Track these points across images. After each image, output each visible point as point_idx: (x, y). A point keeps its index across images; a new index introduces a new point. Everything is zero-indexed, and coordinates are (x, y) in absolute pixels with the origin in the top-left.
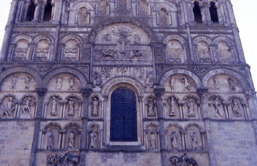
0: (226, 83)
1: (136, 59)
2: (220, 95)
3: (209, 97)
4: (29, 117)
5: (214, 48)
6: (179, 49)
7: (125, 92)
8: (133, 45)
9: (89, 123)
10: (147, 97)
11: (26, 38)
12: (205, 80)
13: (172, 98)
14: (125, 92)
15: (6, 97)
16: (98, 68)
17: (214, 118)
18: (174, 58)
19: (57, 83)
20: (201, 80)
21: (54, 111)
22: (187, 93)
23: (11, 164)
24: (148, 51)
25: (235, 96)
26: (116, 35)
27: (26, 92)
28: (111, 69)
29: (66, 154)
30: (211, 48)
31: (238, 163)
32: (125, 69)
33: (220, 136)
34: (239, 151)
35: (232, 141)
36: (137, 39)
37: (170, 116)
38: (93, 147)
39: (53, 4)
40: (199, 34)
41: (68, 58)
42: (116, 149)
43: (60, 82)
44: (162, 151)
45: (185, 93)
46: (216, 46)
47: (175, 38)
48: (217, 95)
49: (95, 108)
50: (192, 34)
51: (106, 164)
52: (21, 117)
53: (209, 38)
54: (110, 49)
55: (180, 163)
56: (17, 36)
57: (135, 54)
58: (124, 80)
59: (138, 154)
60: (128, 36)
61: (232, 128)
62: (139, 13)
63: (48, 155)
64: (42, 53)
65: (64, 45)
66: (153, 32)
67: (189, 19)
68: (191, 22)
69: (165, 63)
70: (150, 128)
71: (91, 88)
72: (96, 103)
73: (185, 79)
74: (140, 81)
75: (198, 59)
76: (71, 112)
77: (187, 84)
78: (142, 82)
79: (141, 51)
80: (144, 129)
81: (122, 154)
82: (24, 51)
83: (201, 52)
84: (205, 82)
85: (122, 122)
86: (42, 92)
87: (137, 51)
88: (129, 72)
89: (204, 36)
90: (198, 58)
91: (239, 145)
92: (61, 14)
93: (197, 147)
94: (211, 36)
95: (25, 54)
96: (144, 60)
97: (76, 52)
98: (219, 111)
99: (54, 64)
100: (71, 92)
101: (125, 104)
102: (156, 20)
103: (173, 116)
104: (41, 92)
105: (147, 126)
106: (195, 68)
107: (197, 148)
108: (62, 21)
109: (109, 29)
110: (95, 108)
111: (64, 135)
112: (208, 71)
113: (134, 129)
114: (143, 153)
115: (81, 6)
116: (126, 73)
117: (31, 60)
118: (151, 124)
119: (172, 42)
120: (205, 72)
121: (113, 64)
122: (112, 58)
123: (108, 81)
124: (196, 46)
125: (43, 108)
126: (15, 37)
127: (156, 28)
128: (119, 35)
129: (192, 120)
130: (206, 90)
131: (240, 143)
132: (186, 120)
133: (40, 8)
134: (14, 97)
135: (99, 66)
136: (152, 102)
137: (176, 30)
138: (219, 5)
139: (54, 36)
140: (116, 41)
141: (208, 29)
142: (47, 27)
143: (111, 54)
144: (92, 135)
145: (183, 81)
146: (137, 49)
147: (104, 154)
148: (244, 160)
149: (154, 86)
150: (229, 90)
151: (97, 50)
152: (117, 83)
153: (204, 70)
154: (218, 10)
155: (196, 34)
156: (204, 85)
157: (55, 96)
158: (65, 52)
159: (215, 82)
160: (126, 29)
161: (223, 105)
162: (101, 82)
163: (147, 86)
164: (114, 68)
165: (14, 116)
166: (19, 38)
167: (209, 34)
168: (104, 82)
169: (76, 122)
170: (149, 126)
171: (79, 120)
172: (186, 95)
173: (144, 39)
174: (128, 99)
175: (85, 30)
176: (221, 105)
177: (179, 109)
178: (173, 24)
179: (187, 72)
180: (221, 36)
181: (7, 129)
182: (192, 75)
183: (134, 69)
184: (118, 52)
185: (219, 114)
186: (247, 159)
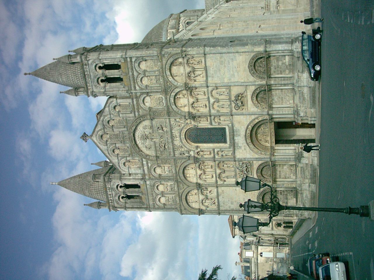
0: (177, 68)
1: (165, 129)
2: (187, 73)
3: (189, 81)
4: (216, 190)
6: (150, 98)
8: (153, 130)
9: (216, 157)
12: (177, 84)
15: (203, 204)
17: (205, 79)
18: (159, 102)
19: (190, 177)
20: (177, 87)
21: (210, 177)
22: (188, 96)
24: (157, 120)
27: (199, 194)
28: (175, 145)
29: (238, 169)
31: (235, 68)
32: (174, 136)
33: (218, 77)
37: (206, 107)
38: (232, 154)
40: (136, 83)
41: (169, 171)
42: (232, 141)
44: (232, 115)
45: (188, 97)
46: (145, 71)
47: (142, 101)
48: (187, 75)
49: (205, 153)
50: (137, 89)
52: (216, 194)
54: (159, 146)
55: (239, 105)
56: (157, 205)
58: (183, 136)
59: (235, 128)
60: (145, 134)
61: (211, 68)
62: (122, 126)
64: (168, 187)
65: (160, 175)
70: (216, 121)
72: (201, 153)
74: (182, 126)
76: (210, 166)
77: (181, 96)
78: (183, 125)
79: (157, 125)
82: (167, 198)
86: (199, 186)
88: (176, 132)
90: (157, 85)
92: (133, 179)
94: (135, 74)
95: (169, 197)
96: (165, 123)
97: (164, 166)
98: (199, 74)
101: (200, 135)
102: (127, 115)
104: (199, 186)
105: (216, 122)
107: (228, 93)
108: (139, 178)
109: (141, 146)
110: (205, 153)
111: (226, 170)
112: (169, 81)
113: (217, 129)
115: (123, 166)
117: (174, 194)
119: (145, 102)
120: (171, 84)
121: (171, 144)
122: (166, 144)
123: (185, 147)
124: (147, 86)
125: (208, 183)
126: (158, 206)
127: (135, 114)
128: (146, 140)
129: (208, 94)
130: (186, 84)
131: (221, 64)
132: (209, 98)
133: (129, 192)
135: (174, 153)
137: (135, 100)
139: (154, 182)
140: (151, 142)
141: (129, 76)
142: (147, 187)
143: (164, 145)
144: (224, 155)
146: (156, 128)
147: (236, 148)
148: (233, 63)
152: (185, 140)
153: (168, 84)
154: (106, 64)
155: (136, 85)
158: (165, 173)
159: (177, 76)
161: (194, 71)
163: (186, 122)
165: (215, 198)
166: (158, 203)
167: (134, 75)
169: (216, 164)
171: (215, 163)
172: (189, 97)
173: (147, 123)
176: (194, 72)
177: (200, 101)
178: (128, 102)
180: (134, 66)
182: (174, 93)
183: (173, 130)
185: (201, 74)
186: (233, 61)
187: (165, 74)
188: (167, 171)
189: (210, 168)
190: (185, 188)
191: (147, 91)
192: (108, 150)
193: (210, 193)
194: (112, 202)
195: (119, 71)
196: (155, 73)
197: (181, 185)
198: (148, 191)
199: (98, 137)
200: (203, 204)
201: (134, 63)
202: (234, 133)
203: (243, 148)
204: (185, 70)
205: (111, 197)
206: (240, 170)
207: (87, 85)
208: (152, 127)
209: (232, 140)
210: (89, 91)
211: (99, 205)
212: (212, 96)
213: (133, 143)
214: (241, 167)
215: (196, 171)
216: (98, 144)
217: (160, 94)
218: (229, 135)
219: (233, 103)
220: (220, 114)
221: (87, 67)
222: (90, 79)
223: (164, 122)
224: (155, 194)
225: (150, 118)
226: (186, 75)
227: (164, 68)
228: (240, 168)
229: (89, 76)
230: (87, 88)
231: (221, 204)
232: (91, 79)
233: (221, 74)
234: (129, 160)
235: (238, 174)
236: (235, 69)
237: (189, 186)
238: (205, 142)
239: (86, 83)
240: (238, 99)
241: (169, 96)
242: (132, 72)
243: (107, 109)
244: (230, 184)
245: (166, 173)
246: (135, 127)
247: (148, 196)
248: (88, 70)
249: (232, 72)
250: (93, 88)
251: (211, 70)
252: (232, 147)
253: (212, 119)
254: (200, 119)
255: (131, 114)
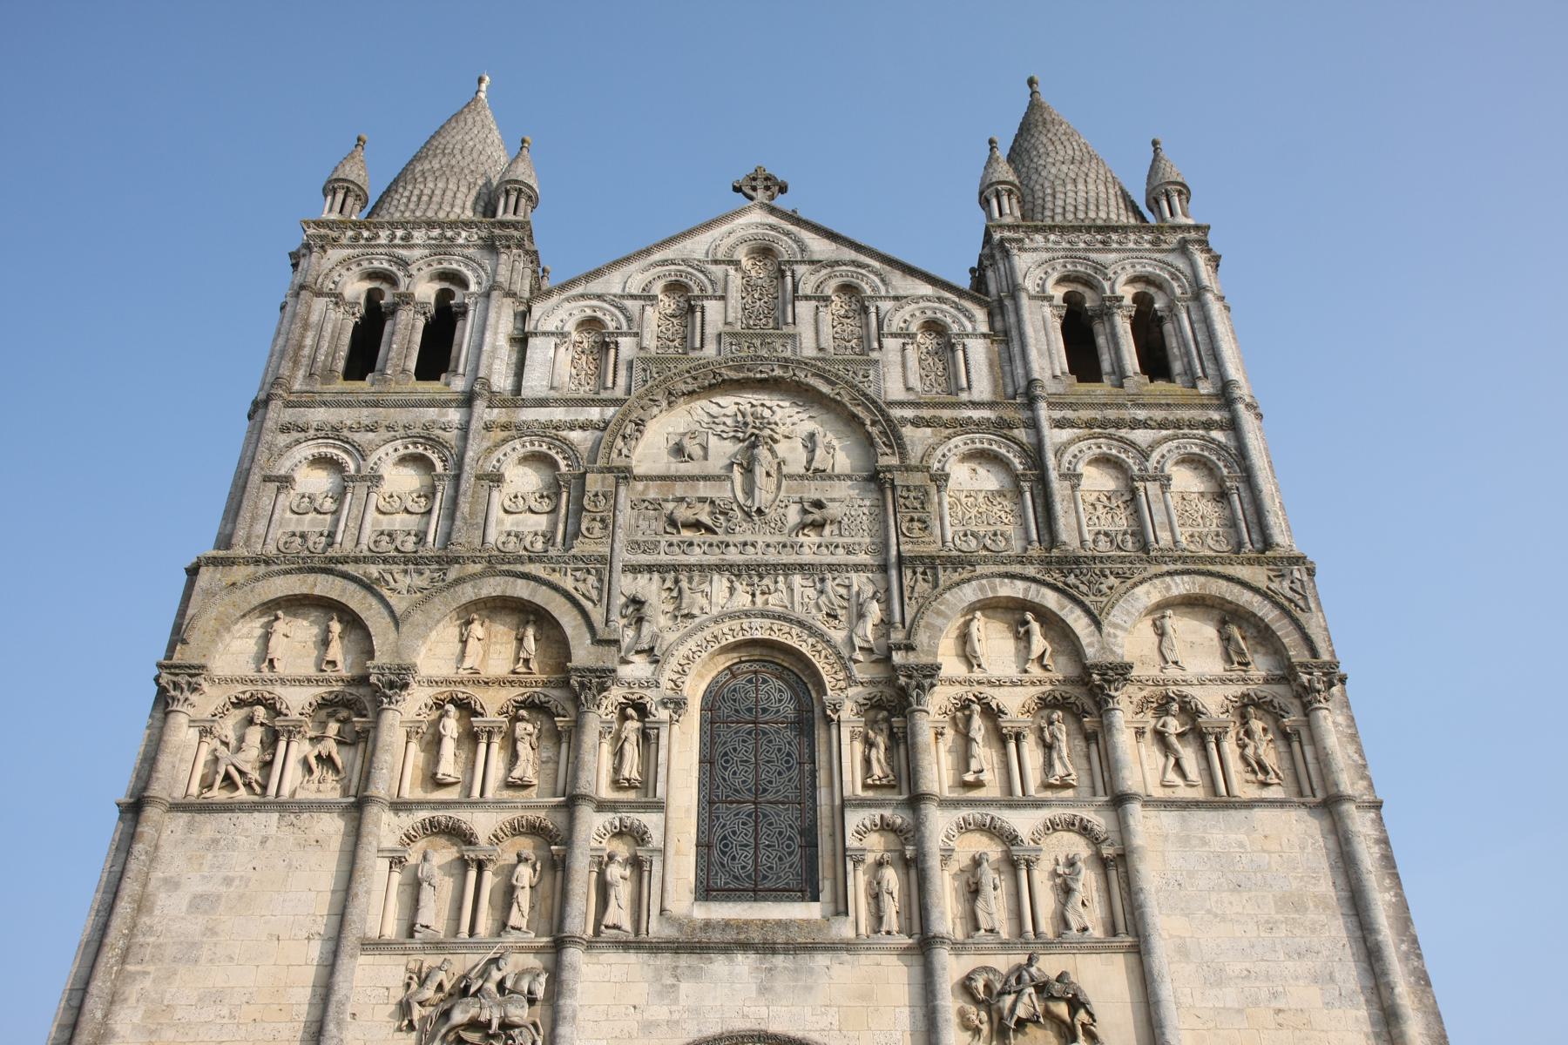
0: (1212, 640)
1: (811, 538)
2: (1186, 690)
3: (1135, 700)
5: (1153, 488)
7: (765, 681)
8: (801, 477)
10: (862, 701)
11: (335, 451)
12: (1115, 626)
13: (976, 708)
14: (765, 681)
16: (647, 576)
17: (1158, 793)
18: (982, 530)
20: (1098, 624)
23: (245, 1007)
25: (1252, 694)
26: (725, 435)
27: (328, 681)
30: (1142, 489)
31: (1275, 995)
32: (766, 581)
34: (1277, 941)
35: (1245, 895)
36: (818, 452)
38: (616, 927)
39: (462, 310)
40: (1086, 431)
42: (716, 936)
43: (479, 640)
45: (1033, 683)
46: (1165, 482)
47: (986, 446)
51: (674, 1008)
53: (1132, 444)
54: (702, 494)
55: (1008, 1000)
56: (298, 442)
57: (810, 518)
58: (760, 630)
59: (821, 960)
61: (1242, 837)
63: (412, 965)
66: (888, 420)
67: (1046, 363)
68: (1055, 377)
69: (942, 553)
71: (610, 666)
73: (1027, 623)
75: (1089, 537)
77: (1039, 643)
78: (838, 636)
79: (837, 504)
80: (848, 844)
81: (748, 961)
83: (1099, 507)
84: (1119, 632)
85: (749, 815)
87: (819, 505)
89: (1110, 437)
90: (1085, 529)
91: (1277, 913)
93: (1089, 925)
94: (1141, 436)
99: (456, 560)
100: (521, 684)
101: (765, 733)
103: (978, 784)
104: (392, 685)
105: (861, 834)
106: (1072, 575)
107: (1085, 929)
112: (1135, 585)
114: (845, 956)
116: (772, 599)
117: (358, 543)
118: (878, 821)
121: (713, 558)
124: (1073, 477)
126: (289, 447)
127: (902, 404)
129: (1064, 803)
130: (1121, 672)
132: (1038, 804)
134: (272, 707)
135: (650, 569)
136: (884, 726)
138: (1171, 308)
143: (706, 519)
145: (1022, 630)
146: (815, 496)
147: (665, 960)
148: (1301, 983)
149: (894, 653)
150: (1225, 670)
151: (644, 501)
152: (731, 640)
153: (1112, 580)
154: (1168, 327)
155: (1075, 430)
156: (1115, 649)
157: (452, 701)
158: (506, 511)
160: (770, 408)
162: (655, 637)
164: (716, 577)
168: (671, 637)
170: (867, 831)
174: (778, 711)
175: (594, 413)
176: (1190, 737)
178: (974, 384)
179: (1038, 592)
180: (1185, 436)
181: (233, 846)
183: (805, 583)
184: (735, 508)
185: (1184, 775)
186: (1315, 980)
187: (1172, 567)
188: (517, 524)
189: (516, 773)
190: (393, 600)
191: (1053, 475)
192: (683, 261)
193: (313, 762)
194: (362, 242)
195: (1135, 373)
196: (1163, 529)
197: (419, 581)
198: (401, 406)
199: (768, 235)
200: (239, 704)
201: (1202, 437)
202: (786, 951)
203: (659, 1012)
204: (1202, 683)
205: (391, 240)
206: (484, 974)
207: (1052, 229)
208: (820, 474)
209: (730, 936)
210: (1021, 235)
211: (351, 187)
212: (1053, 826)
213: (723, 371)
214: (509, 984)
215: (501, 682)
216: (725, 228)
217: (1034, 536)
218: (765, 921)
219: (1023, 959)
220: (934, 862)
221: (1147, 246)
222: (1082, 245)
223: (857, 539)
224: (370, 442)
225: (889, 469)
226: (1175, 688)
227: (1210, 567)
228: (496, 975)
229: (1101, 246)
230: (1037, 230)
231: (210, 825)
232: (1086, 250)
233: (1214, 897)
234: (617, 344)
235: (448, 957)
236: (1264, 994)
237: (396, 621)
238: (707, 760)
239: (1063, 229)
240: (1052, 998)
241: (1038, 576)
242: (1153, 423)
243: (927, 289)
244: (368, 892)
245: (509, 522)
246: (825, 388)
247: (367, 404)
248: (1131, 245)
249: (1236, 967)
250: (1035, 250)
251: (1232, 836)
252: (669, 932)
253: (887, 813)
254: (881, 741)
255: (902, 385)
